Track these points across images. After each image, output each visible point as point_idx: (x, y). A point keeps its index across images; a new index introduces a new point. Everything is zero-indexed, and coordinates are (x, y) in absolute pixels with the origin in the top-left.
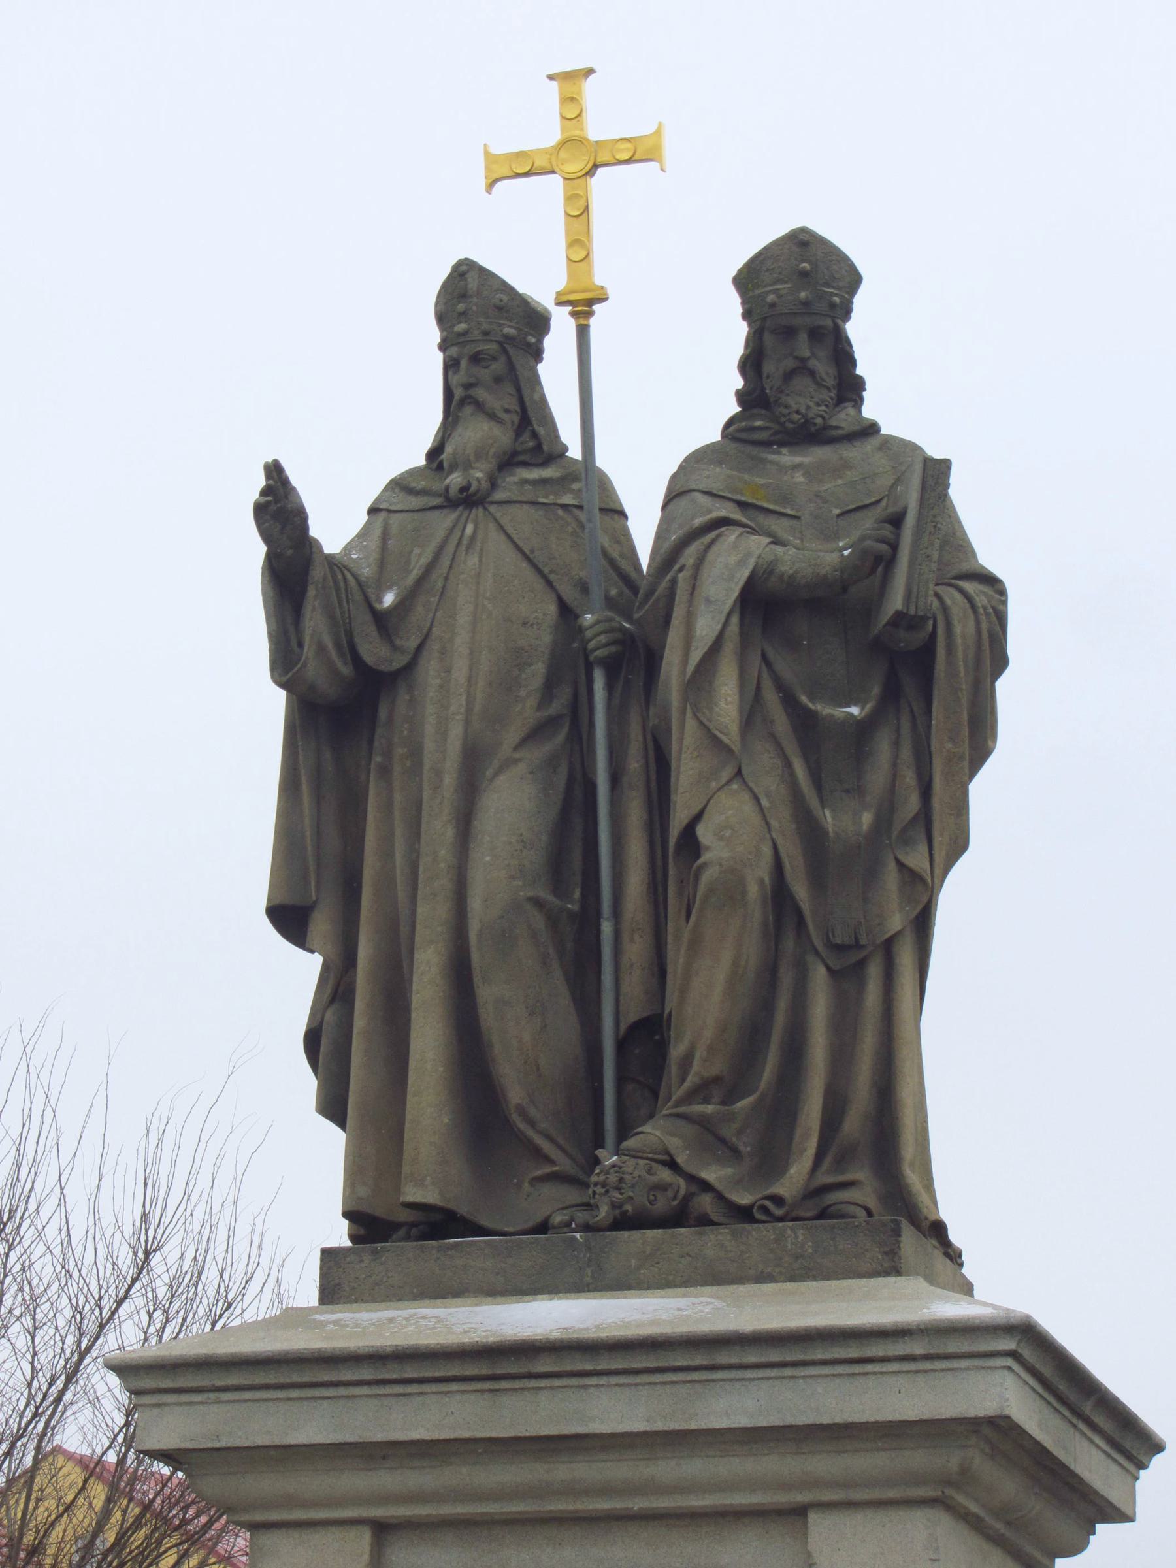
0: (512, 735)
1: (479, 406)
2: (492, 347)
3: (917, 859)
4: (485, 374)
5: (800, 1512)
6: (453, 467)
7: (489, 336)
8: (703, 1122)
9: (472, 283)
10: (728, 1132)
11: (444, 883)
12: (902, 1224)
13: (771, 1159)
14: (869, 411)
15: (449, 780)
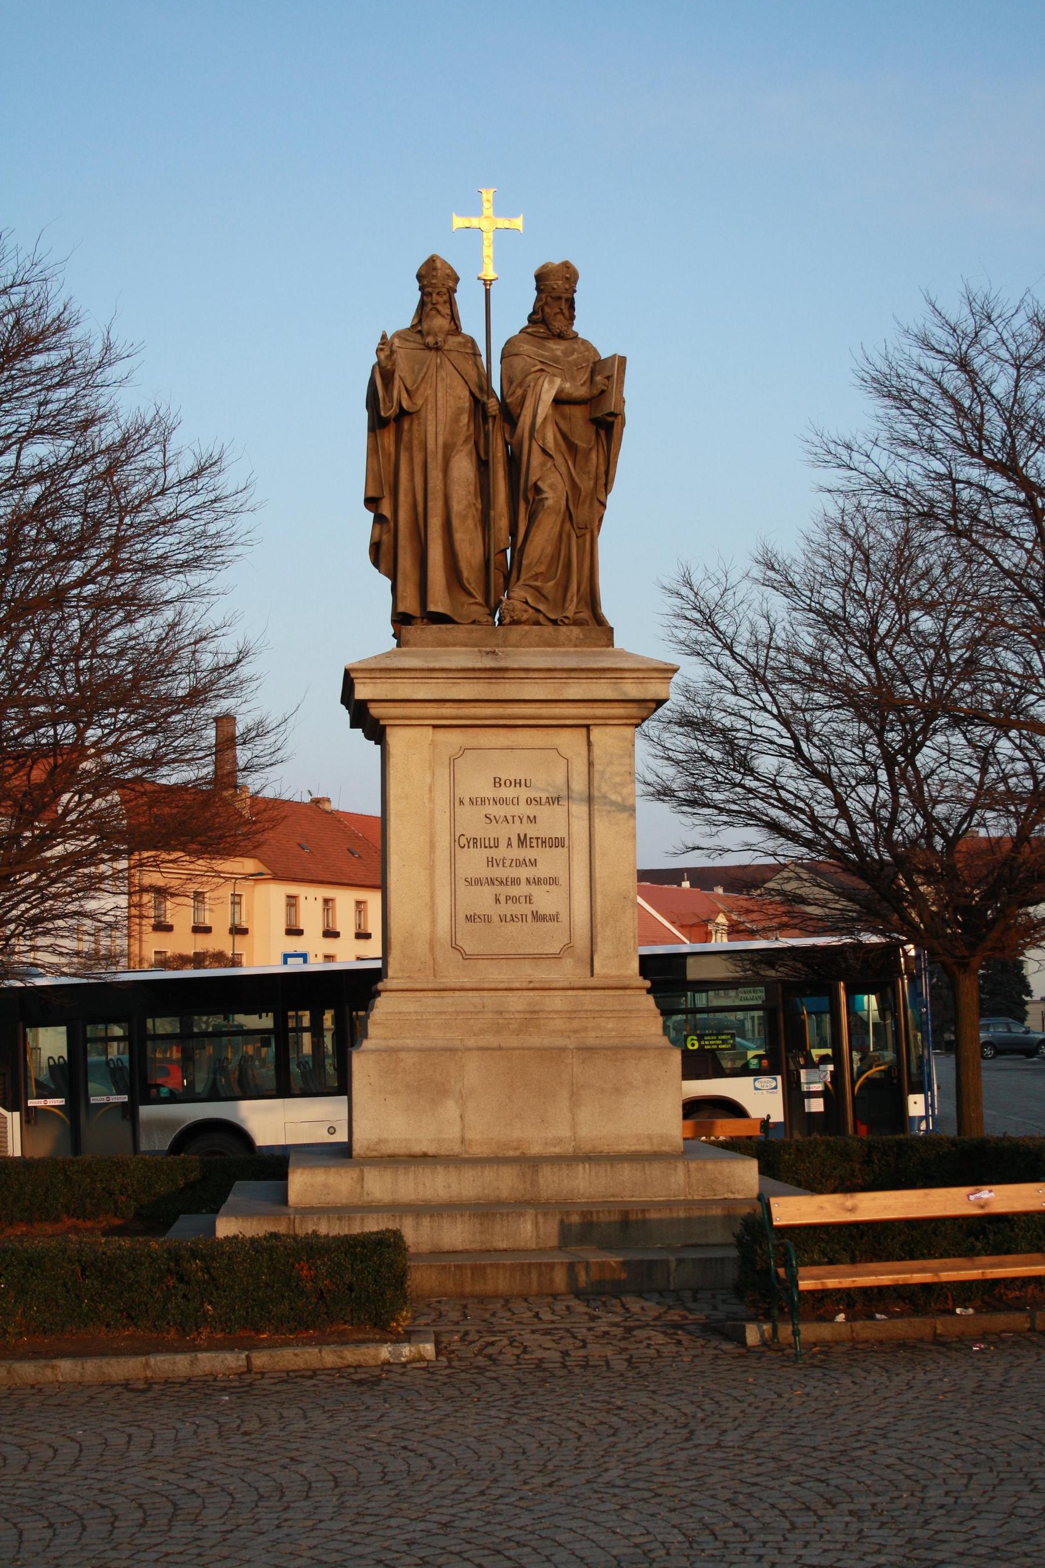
0: (462, 438)
1: (438, 311)
2: (444, 290)
3: (602, 498)
4: (441, 300)
5: (588, 727)
6: (428, 334)
7: (436, 284)
8: (537, 589)
9: (438, 265)
10: (545, 592)
11: (440, 495)
13: (562, 602)
14: (575, 328)
15: (440, 455)
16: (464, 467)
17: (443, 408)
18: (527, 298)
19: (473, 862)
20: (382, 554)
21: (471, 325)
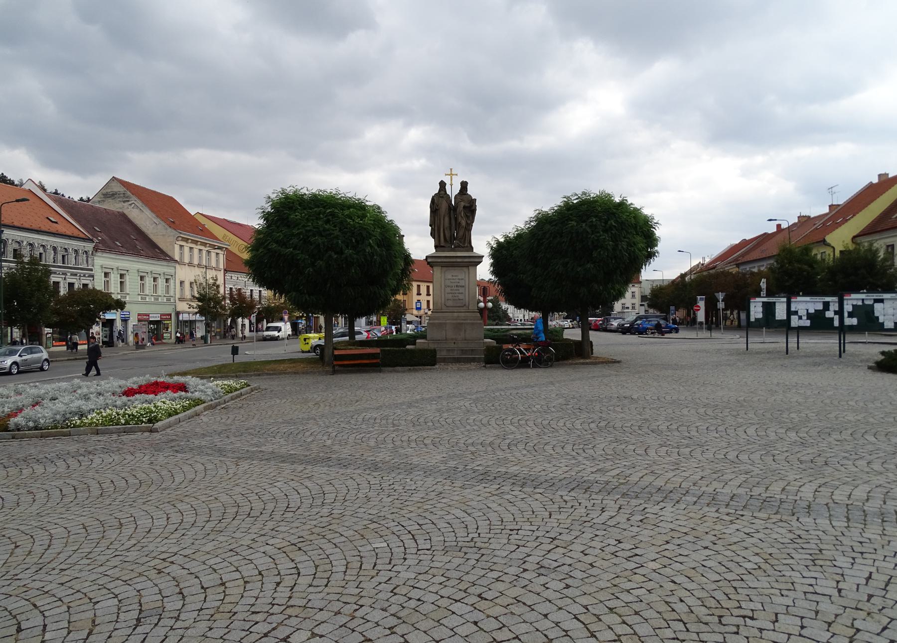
12: (471, 249)
16: (447, 219)
17: (444, 206)
18: (459, 187)
19: (448, 290)
20: (433, 234)
21: (449, 192)
